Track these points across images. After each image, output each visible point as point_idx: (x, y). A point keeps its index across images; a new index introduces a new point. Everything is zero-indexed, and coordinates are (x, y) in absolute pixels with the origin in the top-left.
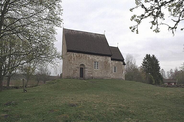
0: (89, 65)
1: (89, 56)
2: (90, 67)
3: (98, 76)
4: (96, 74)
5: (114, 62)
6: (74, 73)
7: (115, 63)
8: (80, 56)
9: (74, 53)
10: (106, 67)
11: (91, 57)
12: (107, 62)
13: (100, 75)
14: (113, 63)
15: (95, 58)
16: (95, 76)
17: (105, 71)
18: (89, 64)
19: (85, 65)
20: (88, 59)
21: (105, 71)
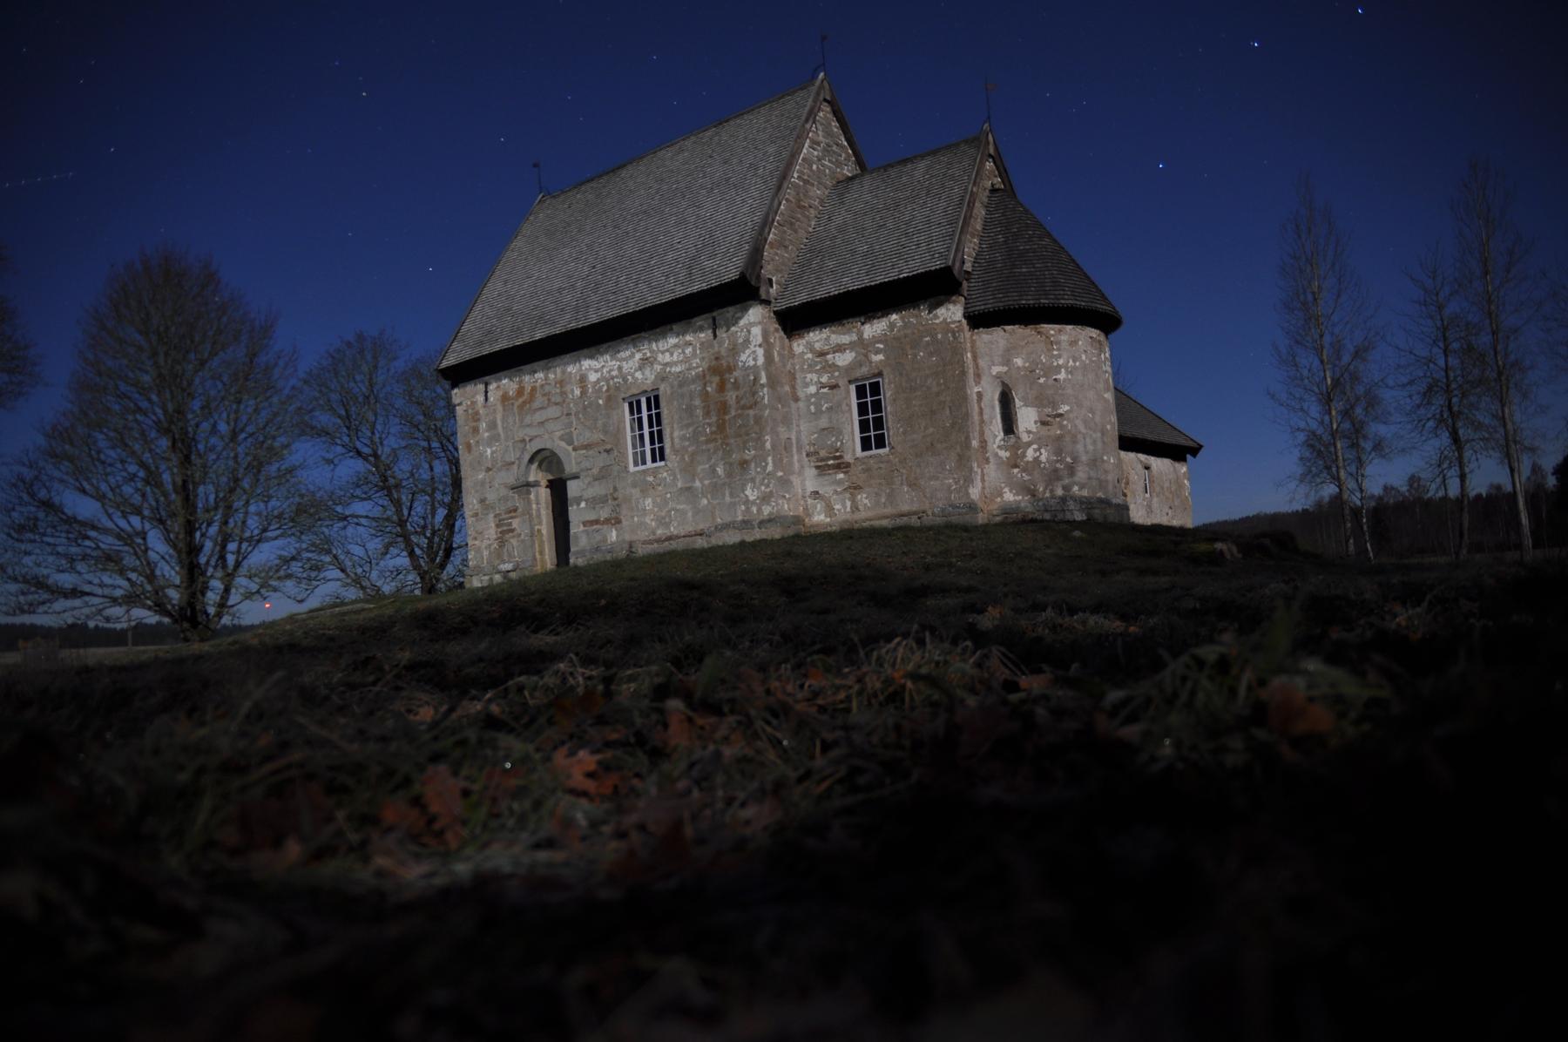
0: (587, 447)
1: (586, 363)
2: (602, 460)
3: (667, 525)
4: (647, 520)
5: (845, 339)
6: (502, 542)
7: (852, 346)
10: (721, 427)
11: (594, 368)
12: (730, 369)
13: (684, 513)
14: (840, 349)
16: (643, 535)
17: (720, 470)
18: (588, 436)
19: (561, 448)
20: (577, 392)
21: (720, 470)
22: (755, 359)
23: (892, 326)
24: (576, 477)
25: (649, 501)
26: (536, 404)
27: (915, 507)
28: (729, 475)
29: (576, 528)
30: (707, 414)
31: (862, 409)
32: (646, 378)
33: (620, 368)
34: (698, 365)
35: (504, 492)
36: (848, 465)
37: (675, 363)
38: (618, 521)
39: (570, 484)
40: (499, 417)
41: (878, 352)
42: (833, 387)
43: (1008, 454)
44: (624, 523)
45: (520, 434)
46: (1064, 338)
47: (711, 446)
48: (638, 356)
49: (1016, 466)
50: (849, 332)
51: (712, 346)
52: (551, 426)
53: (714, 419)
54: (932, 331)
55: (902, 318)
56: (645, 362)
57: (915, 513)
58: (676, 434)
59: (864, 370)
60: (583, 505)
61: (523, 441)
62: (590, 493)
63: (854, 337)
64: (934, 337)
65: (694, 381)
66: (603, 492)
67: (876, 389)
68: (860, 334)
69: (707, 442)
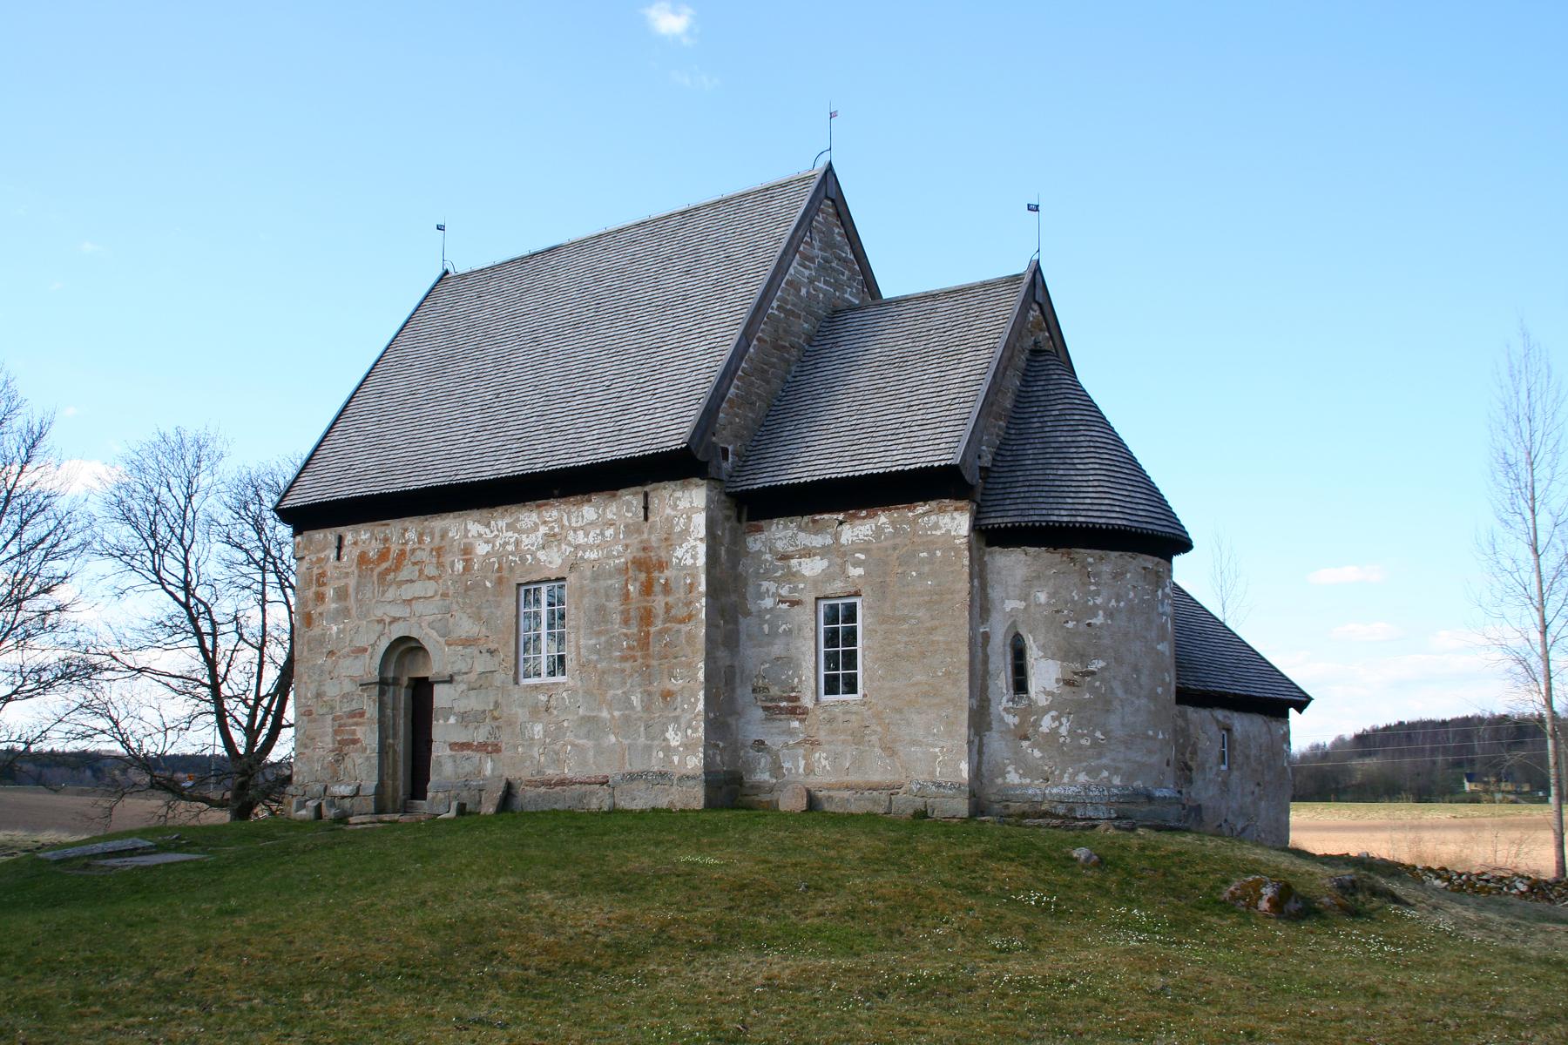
1: (474, 528)
2: (482, 664)
4: (535, 752)
5: (817, 541)
6: (340, 756)
7: (824, 552)
8: (395, 548)
9: (341, 530)
10: (644, 642)
11: (482, 535)
12: (661, 566)
14: (808, 553)
15: (528, 532)
17: (636, 700)
20: (459, 566)
21: (636, 700)
22: (694, 557)
23: (879, 530)
24: (450, 680)
25: (538, 728)
26: (404, 574)
27: (888, 778)
28: (647, 708)
29: (440, 751)
30: (626, 622)
31: (832, 638)
32: (553, 560)
33: (517, 543)
34: (620, 555)
35: (348, 687)
36: (805, 712)
37: (591, 547)
38: (497, 749)
39: (437, 689)
40: (352, 582)
41: (857, 564)
42: (794, 603)
43: (1016, 720)
44: (506, 753)
45: (379, 613)
46: (1106, 568)
47: (627, 665)
48: (543, 530)
49: (1026, 738)
50: (818, 530)
51: (640, 532)
52: (419, 607)
53: (635, 630)
54: (930, 545)
55: (893, 523)
56: (551, 539)
57: (888, 787)
58: (582, 642)
59: (838, 586)
60: (452, 720)
61: (380, 621)
62: (461, 706)
63: (829, 540)
64: (932, 554)
65: (611, 576)
66: (480, 707)
67: (851, 614)
68: (837, 536)
69: (624, 659)
